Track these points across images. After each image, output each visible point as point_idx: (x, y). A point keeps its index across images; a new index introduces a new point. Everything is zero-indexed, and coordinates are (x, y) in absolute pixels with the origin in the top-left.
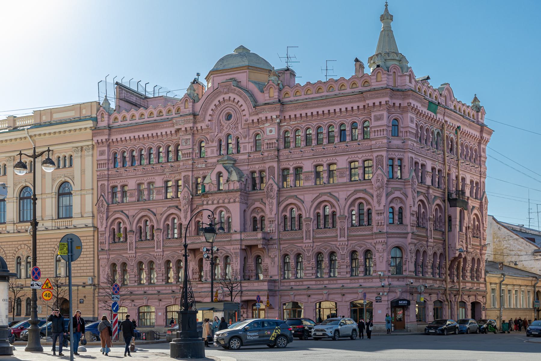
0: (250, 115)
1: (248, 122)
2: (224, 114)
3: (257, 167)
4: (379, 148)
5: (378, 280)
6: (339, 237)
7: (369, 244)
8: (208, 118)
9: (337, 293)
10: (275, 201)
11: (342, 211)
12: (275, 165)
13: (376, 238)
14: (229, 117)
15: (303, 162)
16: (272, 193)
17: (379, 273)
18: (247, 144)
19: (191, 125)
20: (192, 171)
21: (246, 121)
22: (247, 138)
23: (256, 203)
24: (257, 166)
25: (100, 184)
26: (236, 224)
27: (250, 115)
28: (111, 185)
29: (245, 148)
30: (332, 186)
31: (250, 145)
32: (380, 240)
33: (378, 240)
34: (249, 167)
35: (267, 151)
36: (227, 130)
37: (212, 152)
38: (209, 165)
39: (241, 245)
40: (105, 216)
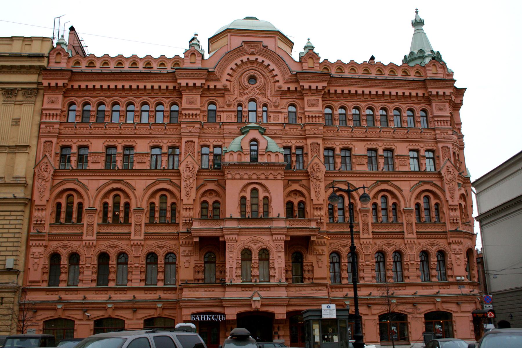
0: (286, 82)
1: (283, 89)
2: (245, 77)
3: (293, 143)
4: (444, 138)
5: (456, 287)
6: (406, 234)
7: (442, 244)
8: (225, 77)
9: (408, 303)
10: (323, 185)
11: (407, 203)
12: (320, 142)
13: (452, 237)
14: (253, 79)
15: (354, 143)
16: (318, 174)
17: (458, 278)
18: (280, 115)
19: (204, 81)
20: (199, 137)
21: (280, 87)
22: (279, 108)
23: (293, 184)
24: (293, 141)
25: (43, 140)
26: (278, 208)
27: (286, 82)
28: (62, 144)
29: (276, 118)
30: (380, 174)
31: (283, 116)
32: (457, 239)
33: (454, 239)
34: (283, 141)
35: (309, 124)
36: (251, 95)
37: (229, 117)
38: (225, 131)
39: (287, 235)
40: (49, 185)
